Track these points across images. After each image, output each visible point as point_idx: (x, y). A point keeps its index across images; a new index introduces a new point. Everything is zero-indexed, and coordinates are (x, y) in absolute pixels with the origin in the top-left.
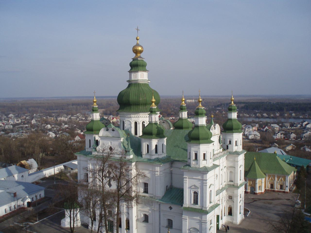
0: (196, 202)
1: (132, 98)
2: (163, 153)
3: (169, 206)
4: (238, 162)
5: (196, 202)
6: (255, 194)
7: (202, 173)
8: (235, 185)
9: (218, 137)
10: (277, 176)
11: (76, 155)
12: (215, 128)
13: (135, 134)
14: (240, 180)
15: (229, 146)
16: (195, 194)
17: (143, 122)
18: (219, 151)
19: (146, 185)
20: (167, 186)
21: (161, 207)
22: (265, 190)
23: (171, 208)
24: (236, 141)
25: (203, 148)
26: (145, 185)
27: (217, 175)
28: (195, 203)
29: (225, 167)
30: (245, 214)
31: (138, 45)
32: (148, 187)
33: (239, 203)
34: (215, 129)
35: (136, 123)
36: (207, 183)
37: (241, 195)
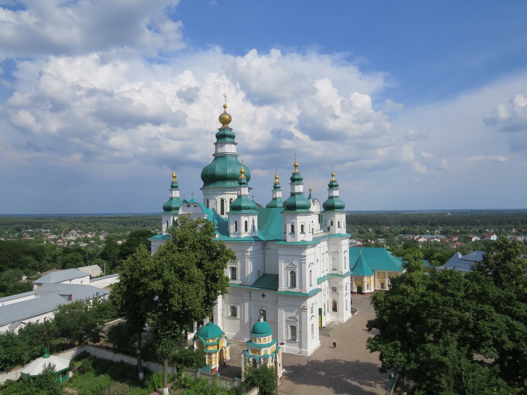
0: (293, 285)
1: (219, 170)
2: (254, 232)
3: (261, 293)
4: (341, 246)
5: (293, 285)
6: (362, 294)
7: (300, 248)
8: (339, 274)
9: (318, 215)
10: (388, 273)
11: (151, 240)
12: (314, 204)
13: (221, 214)
14: (345, 269)
15: (331, 228)
16: (292, 274)
17: (231, 199)
18: (319, 232)
19: (234, 270)
20: (259, 271)
21: (251, 295)
22: (375, 290)
23: (264, 296)
24: (339, 222)
25: (300, 220)
26: (232, 270)
27: (317, 260)
28: (293, 285)
29: (326, 253)
30: (353, 311)
31: (225, 113)
32: (236, 272)
33: (345, 296)
34: (314, 205)
35: (222, 201)
36: (306, 260)
37: (346, 286)
